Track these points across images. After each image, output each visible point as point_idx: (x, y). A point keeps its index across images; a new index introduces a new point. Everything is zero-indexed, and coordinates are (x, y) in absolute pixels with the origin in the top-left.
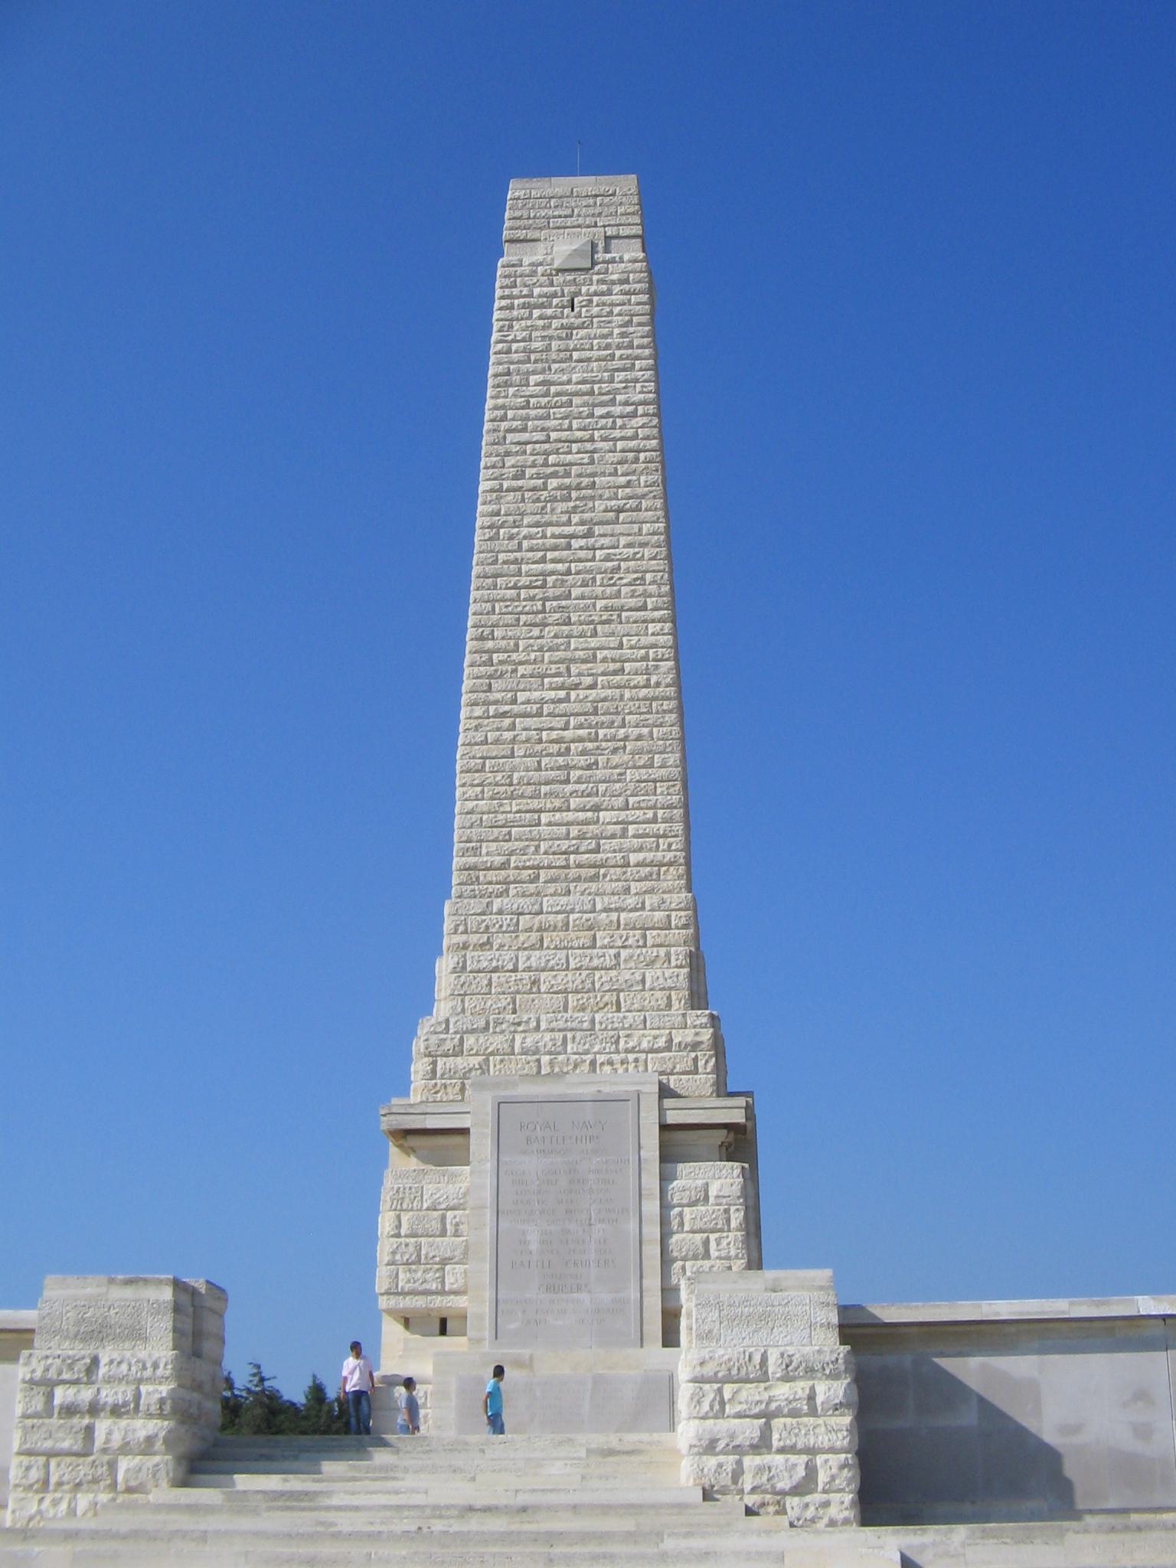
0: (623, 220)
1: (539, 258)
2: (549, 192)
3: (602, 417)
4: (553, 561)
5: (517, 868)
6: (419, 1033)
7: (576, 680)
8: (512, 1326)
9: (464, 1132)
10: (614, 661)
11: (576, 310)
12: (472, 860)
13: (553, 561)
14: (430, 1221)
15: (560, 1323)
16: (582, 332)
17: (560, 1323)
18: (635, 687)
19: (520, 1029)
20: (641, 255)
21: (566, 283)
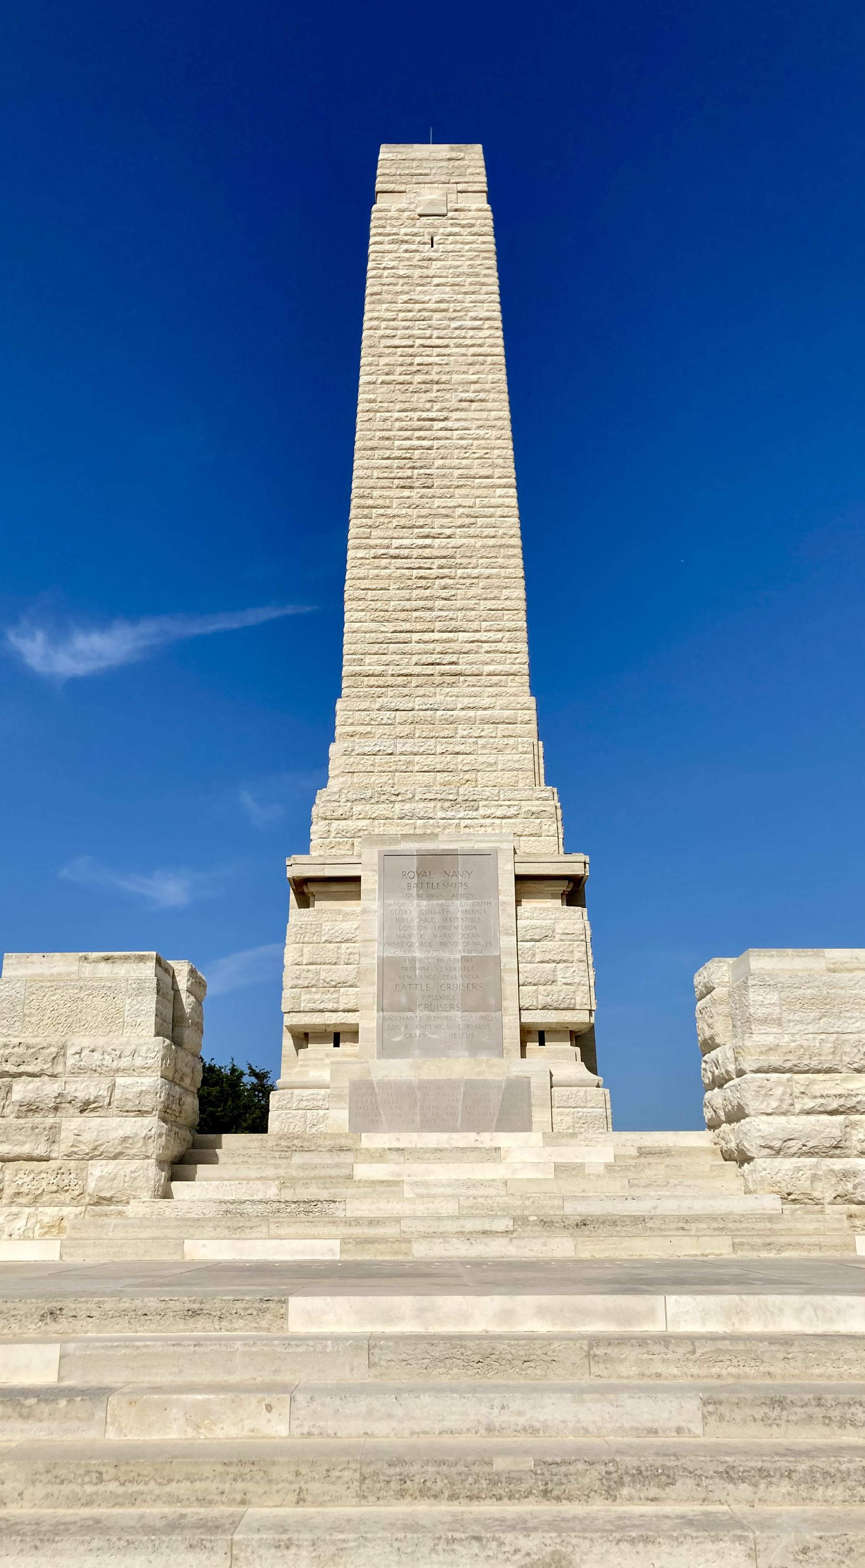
0: (471, 178)
1: (403, 206)
2: (412, 156)
3: (456, 329)
4: (419, 438)
5: (393, 675)
6: (317, 801)
7: (439, 531)
8: (397, 1039)
9: (357, 879)
10: (468, 516)
11: (435, 246)
12: (358, 669)
13: (419, 438)
14: (327, 956)
15: (436, 1036)
16: (439, 264)
17: (436, 1036)
18: (486, 537)
19: (400, 798)
20: (488, 206)
21: (425, 226)
